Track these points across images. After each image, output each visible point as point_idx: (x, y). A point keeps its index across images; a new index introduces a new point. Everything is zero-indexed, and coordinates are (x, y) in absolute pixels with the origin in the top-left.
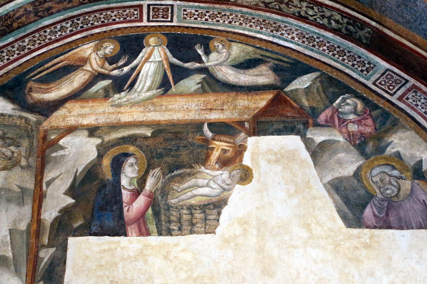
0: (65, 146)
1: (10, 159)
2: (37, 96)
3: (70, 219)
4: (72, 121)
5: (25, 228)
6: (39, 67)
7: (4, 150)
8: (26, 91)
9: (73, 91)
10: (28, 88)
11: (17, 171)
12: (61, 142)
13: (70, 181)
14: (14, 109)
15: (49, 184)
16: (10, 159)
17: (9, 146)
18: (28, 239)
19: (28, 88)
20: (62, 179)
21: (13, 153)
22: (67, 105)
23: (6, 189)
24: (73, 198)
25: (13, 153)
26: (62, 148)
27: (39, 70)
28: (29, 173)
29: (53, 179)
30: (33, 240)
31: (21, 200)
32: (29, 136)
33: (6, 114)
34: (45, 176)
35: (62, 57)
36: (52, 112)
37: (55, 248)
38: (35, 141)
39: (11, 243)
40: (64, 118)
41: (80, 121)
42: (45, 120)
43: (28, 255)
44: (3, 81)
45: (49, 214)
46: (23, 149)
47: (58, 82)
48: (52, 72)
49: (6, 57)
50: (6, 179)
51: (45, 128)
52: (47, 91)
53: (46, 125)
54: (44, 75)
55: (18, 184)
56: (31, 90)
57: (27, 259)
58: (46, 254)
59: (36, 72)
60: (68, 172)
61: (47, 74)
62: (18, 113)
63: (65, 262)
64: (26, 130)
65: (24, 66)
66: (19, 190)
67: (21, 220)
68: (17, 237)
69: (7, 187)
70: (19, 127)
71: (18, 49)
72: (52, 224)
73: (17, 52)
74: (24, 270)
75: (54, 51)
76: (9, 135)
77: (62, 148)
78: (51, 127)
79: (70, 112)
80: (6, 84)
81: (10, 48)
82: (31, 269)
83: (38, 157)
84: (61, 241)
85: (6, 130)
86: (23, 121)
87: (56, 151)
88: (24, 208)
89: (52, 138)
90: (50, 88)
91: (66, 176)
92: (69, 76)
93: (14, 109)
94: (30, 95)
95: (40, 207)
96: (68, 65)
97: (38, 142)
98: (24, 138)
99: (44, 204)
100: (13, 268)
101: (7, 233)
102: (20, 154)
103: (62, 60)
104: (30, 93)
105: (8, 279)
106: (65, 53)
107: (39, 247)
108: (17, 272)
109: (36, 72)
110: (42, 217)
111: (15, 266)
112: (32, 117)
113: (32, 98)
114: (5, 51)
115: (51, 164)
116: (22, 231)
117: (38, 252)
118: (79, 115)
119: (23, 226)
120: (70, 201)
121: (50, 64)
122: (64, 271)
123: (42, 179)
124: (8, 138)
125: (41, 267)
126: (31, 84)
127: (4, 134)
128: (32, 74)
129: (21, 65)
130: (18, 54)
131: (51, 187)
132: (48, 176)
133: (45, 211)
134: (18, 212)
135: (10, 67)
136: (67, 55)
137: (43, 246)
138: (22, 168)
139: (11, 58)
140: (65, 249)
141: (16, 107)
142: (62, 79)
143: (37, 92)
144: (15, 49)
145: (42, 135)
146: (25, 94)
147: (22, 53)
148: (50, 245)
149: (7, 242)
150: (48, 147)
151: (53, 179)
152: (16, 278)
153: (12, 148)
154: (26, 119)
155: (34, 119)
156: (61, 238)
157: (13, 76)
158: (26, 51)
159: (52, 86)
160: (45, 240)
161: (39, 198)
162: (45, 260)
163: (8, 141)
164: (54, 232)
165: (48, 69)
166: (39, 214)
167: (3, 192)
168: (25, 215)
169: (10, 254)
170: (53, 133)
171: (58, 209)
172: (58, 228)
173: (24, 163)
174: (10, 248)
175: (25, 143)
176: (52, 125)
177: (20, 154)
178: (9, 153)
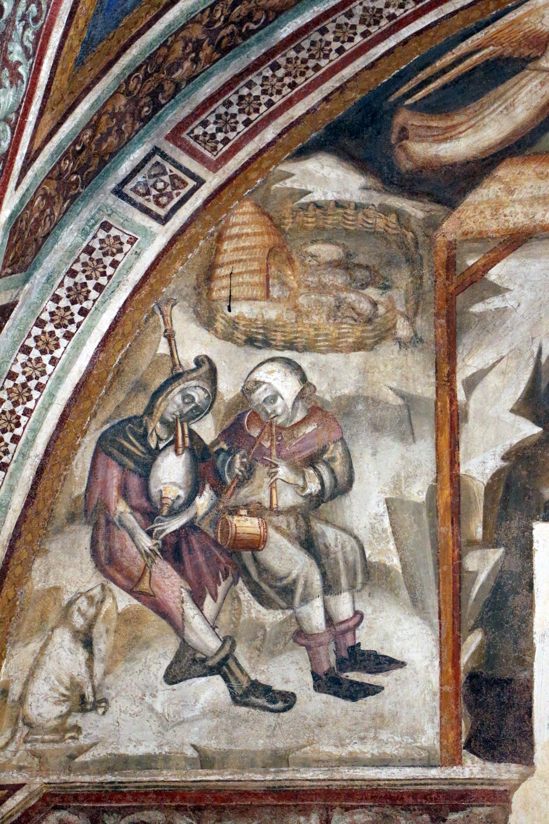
0: (505, 285)
1: (369, 321)
2: (423, 150)
3: (533, 475)
4: (517, 216)
5: (422, 498)
6: (422, 69)
7: (352, 297)
8: (394, 138)
9: (514, 133)
10: (396, 130)
11: (389, 352)
12: (493, 275)
13: (526, 376)
14: (365, 188)
15: (471, 384)
16: (369, 321)
17: (364, 286)
18: (432, 525)
19: (396, 130)
20: (503, 373)
21: (375, 304)
22: (503, 172)
23: (366, 398)
24: (537, 422)
25: (375, 304)
26: (497, 290)
27: (422, 76)
28: (419, 357)
29: (481, 374)
30: (446, 529)
31: (405, 426)
32: (410, 261)
33: (349, 203)
34: (460, 364)
35: (479, 37)
36: (464, 192)
37: (501, 550)
38: (425, 271)
39: (394, 533)
40: (497, 208)
41: (538, 217)
42: (448, 215)
43: (437, 564)
44: (331, 113)
45: (481, 464)
46: (398, 295)
47: (474, 106)
48: (456, 82)
49: (336, 45)
50: (364, 372)
51: (450, 238)
52: (446, 135)
53: (449, 229)
54: (437, 91)
55: (394, 385)
56: (404, 134)
57: (437, 575)
58: (482, 564)
59: (413, 83)
60: (517, 353)
61: (444, 87)
62: (377, 199)
63: (531, 585)
64: (402, 245)
65: (382, 66)
66: (400, 401)
67: (411, 478)
68: (406, 518)
69: (369, 393)
70: (383, 236)
71: (362, 21)
72: (489, 489)
73: (361, 29)
74: (432, 601)
75: (458, 20)
76: (361, 259)
77: (497, 290)
78: (465, 234)
79: (511, 192)
80: (340, 121)
81: (341, 19)
82: (449, 599)
83: (437, 315)
84: (515, 532)
85: (351, 244)
86: (393, 218)
87: (482, 299)
88: (414, 447)
89: (470, 262)
90: (454, 127)
91: (513, 364)
92: (501, 89)
93: (365, 188)
94: (404, 149)
95: (454, 445)
96: (499, 59)
97: (435, 275)
98: (398, 266)
99: (463, 438)
100: (404, 594)
101: (383, 508)
102: (391, 309)
103: (481, 46)
104: (404, 142)
105: (398, 622)
106: (487, 24)
107: (463, 546)
108: (416, 604)
109: (413, 83)
110: (462, 471)
111: (411, 589)
112: (414, 209)
113: (409, 158)
114: (331, 27)
115: (473, 333)
116: (417, 505)
117: (460, 557)
118: (535, 200)
119: (418, 492)
120: (530, 430)
121: (449, 58)
122: (531, 606)
123: (452, 372)
124: (359, 266)
125: (474, 594)
126: (403, 118)
127: (348, 255)
128: (404, 89)
129: (373, 65)
130: (364, 34)
131: (477, 394)
132: (468, 365)
133: (469, 456)
134: (403, 457)
135: (348, 72)
136: (492, 30)
137: (473, 544)
138: (402, 343)
139: (347, 46)
140: (527, 552)
141: (371, 182)
142: (484, 99)
143: (422, 139)
144: (355, 21)
145: (443, 256)
146: (392, 147)
147: (374, 30)
148: (489, 542)
149: (384, 531)
150: (462, 288)
151: (481, 374)
152: (417, 619)
153: (372, 292)
154: (399, 214)
155: (420, 215)
156: (514, 524)
157: (355, 96)
158: (384, 23)
159: (457, 119)
160: (476, 529)
161: (450, 423)
162: (482, 578)
163: (360, 274)
164: (497, 509)
165: (444, 71)
166: (454, 463)
167: (360, 407)
168: (419, 466)
169: (394, 562)
170: (471, 251)
171: (501, 450)
172: (505, 501)
173: (403, 330)
174: (392, 546)
175: (403, 279)
176: (465, 228)
177: (391, 309)
178: (365, 307)
